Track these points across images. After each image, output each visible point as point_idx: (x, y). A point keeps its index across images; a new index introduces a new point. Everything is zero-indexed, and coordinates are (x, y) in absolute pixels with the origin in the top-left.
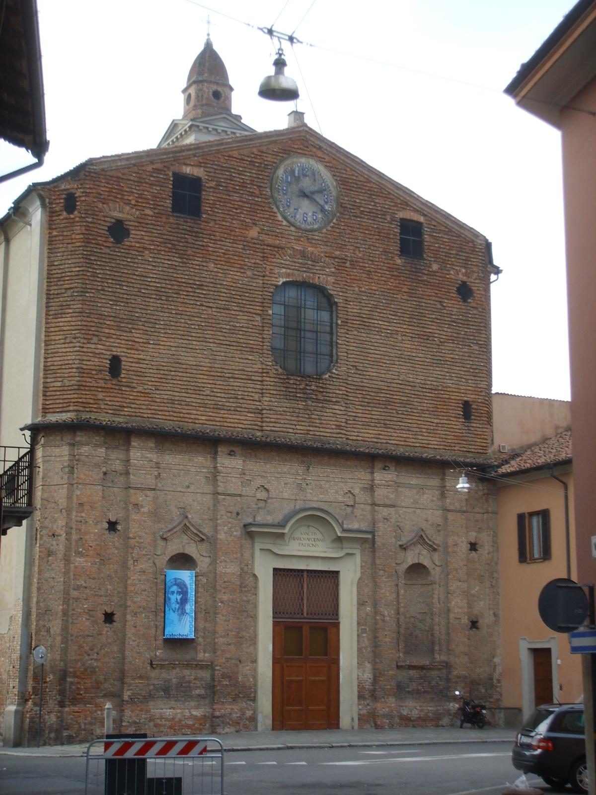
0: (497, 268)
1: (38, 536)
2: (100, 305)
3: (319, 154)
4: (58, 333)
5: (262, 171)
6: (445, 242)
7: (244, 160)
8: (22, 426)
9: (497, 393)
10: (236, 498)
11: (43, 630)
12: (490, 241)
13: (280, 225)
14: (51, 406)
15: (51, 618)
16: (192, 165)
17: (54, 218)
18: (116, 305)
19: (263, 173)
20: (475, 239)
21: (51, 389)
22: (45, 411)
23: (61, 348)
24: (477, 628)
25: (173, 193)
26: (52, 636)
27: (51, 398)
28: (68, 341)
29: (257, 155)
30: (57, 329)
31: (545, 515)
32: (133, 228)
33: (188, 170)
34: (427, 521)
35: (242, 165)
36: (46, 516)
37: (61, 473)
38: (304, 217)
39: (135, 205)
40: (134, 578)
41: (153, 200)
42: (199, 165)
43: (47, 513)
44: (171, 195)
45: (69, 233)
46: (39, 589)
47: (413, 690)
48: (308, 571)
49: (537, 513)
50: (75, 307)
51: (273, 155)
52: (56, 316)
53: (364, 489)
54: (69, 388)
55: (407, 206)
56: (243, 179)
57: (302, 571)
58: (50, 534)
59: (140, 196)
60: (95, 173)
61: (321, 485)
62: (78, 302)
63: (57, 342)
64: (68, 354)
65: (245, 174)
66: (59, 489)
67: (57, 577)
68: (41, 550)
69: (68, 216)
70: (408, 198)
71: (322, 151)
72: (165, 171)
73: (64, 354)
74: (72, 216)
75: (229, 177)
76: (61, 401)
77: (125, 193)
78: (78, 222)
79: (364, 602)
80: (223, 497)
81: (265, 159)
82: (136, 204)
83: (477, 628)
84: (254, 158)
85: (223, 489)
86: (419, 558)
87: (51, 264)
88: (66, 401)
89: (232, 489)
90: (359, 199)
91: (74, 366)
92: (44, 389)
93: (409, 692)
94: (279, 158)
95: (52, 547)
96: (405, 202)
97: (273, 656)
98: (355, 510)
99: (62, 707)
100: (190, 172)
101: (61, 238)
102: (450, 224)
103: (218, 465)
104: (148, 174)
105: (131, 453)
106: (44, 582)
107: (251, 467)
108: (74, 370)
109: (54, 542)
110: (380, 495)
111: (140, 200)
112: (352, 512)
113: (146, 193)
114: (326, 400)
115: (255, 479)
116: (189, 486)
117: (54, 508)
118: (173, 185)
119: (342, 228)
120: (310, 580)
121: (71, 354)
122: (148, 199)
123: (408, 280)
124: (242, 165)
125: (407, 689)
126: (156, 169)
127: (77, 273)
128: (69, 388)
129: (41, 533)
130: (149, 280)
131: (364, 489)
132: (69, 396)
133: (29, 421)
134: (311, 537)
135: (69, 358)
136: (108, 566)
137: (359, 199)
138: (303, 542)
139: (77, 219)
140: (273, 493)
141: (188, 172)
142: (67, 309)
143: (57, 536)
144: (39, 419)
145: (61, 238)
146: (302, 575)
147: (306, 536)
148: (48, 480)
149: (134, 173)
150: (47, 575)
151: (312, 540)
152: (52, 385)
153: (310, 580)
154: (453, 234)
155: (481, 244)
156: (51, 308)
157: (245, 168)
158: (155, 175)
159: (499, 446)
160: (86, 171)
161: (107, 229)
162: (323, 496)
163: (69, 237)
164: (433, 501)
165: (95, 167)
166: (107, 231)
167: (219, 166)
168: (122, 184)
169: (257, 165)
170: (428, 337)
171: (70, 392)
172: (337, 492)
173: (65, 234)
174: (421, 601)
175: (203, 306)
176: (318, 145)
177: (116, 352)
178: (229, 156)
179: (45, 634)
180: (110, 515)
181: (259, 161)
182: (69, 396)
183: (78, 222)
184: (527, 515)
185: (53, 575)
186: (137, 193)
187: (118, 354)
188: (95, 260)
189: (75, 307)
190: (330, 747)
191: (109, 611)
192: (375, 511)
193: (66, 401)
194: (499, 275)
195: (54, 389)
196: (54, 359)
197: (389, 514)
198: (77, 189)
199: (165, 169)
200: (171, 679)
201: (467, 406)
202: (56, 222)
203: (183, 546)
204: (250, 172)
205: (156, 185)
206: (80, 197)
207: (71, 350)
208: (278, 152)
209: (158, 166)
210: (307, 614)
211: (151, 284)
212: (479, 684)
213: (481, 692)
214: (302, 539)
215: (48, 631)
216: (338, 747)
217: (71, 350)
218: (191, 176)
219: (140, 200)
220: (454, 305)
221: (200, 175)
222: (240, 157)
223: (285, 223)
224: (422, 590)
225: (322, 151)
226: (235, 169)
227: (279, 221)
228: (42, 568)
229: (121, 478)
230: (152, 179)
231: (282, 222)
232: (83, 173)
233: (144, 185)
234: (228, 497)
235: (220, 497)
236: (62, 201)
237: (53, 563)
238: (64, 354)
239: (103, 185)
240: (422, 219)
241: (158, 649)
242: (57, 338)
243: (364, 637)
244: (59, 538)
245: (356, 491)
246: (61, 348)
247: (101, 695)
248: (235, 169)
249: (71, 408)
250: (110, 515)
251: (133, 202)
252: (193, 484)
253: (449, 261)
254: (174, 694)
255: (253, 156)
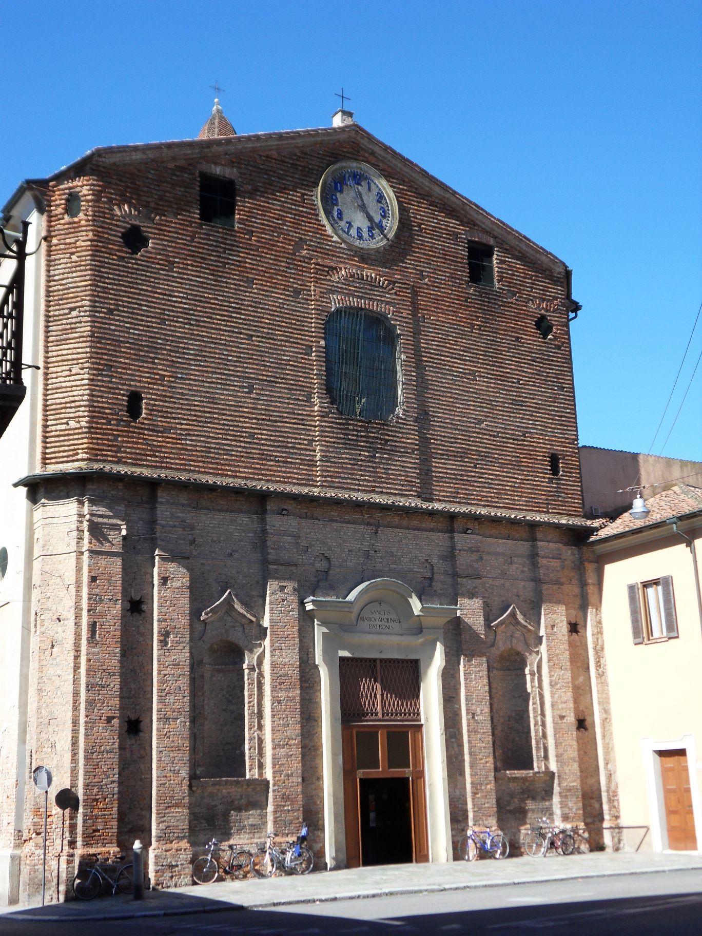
0: (576, 303)
1: (38, 622)
2: (113, 328)
3: (371, 158)
4: (60, 364)
5: (306, 176)
6: (519, 268)
7: (285, 162)
8: (16, 480)
9: (584, 447)
10: (291, 568)
11: (46, 746)
12: (570, 269)
13: (330, 241)
14: (53, 455)
15: (56, 729)
16: (223, 165)
17: (53, 224)
18: (134, 329)
19: (308, 179)
20: (552, 266)
21: (53, 433)
22: (45, 461)
23: (65, 382)
24: (586, 729)
25: (201, 196)
26: (58, 753)
27: (53, 445)
28: (74, 372)
29: (300, 157)
30: (60, 358)
31: (665, 583)
32: (153, 236)
33: (218, 170)
34: (517, 596)
35: (283, 168)
36: (48, 595)
37: (67, 539)
38: (358, 232)
39: (155, 209)
40: (165, 672)
41: (176, 204)
42: (231, 164)
43: (50, 591)
44: (199, 198)
45: (72, 240)
46: (40, 691)
47: (515, 808)
48: (381, 660)
49: (656, 582)
50: (82, 329)
51: (318, 158)
52: (59, 342)
53: (443, 558)
54: (76, 431)
55: (474, 225)
56: (284, 184)
57: (375, 660)
58: (55, 618)
59: (161, 198)
60: (104, 167)
61: (392, 553)
62: (86, 324)
63: (59, 374)
64: (74, 388)
65: (287, 178)
66: (65, 559)
67: (63, 674)
68: (42, 639)
69: (71, 220)
70: (476, 216)
71: (375, 157)
72: (190, 170)
73: (69, 389)
74: (76, 219)
75: (267, 181)
76: (66, 448)
77: (142, 193)
78: (84, 226)
79: (451, 697)
80: (276, 567)
81: (310, 162)
82: (157, 207)
83: (586, 729)
84: (296, 159)
85: (275, 557)
86: (511, 642)
87: (49, 279)
88: (72, 448)
89: (285, 556)
90: (420, 215)
91: (82, 403)
92: (44, 434)
93: (510, 812)
94: (325, 162)
95: (56, 635)
96: (472, 221)
97: (344, 767)
98: (434, 584)
99: (73, 849)
100: (220, 172)
101: (62, 247)
102: (524, 248)
103: (268, 527)
104: (170, 171)
105: (158, 512)
106: (46, 681)
107: (308, 530)
108: (83, 409)
109: (60, 628)
110: (463, 565)
111: (160, 203)
112: (430, 586)
113: (168, 194)
114: (392, 451)
115: (313, 545)
116: (231, 554)
117: (58, 584)
118: (200, 187)
119: (403, 247)
120: (384, 671)
121: (79, 388)
122: (171, 202)
123: (480, 311)
124: (283, 168)
125: (508, 808)
126: (179, 166)
127: (83, 289)
128: (76, 431)
129: (42, 617)
130: (174, 299)
131: (443, 558)
132: (76, 442)
133: (24, 473)
134: (384, 617)
135: (75, 393)
136: (130, 658)
137: (420, 215)
138: (375, 623)
139: (83, 223)
140: (334, 561)
141: (218, 173)
142: (72, 333)
143: (64, 620)
144: (38, 471)
145: (62, 247)
146: (375, 666)
147: (378, 616)
148: (51, 548)
149: (152, 169)
150: (51, 671)
151: (386, 620)
152: (53, 428)
153: (384, 671)
154: (528, 259)
155: (560, 273)
156: (51, 334)
157: (286, 171)
158: (178, 173)
159: (591, 508)
160: (93, 165)
161: (120, 235)
162: (396, 566)
163: (73, 245)
164: (523, 572)
165: (104, 159)
166: (121, 237)
167: (255, 167)
168: (137, 183)
169: (300, 168)
170: (505, 378)
171: (76, 437)
172: (411, 561)
173: (68, 241)
174: (516, 696)
175: (241, 333)
176: (370, 149)
177: (135, 385)
178: (267, 157)
179: (50, 750)
180: (133, 591)
181: (302, 164)
182: (76, 442)
183: (84, 226)
184: (640, 586)
185: (59, 672)
186: (156, 194)
187: (139, 389)
188: (106, 273)
189: (82, 329)
190: (442, 890)
191: (133, 718)
192: (457, 584)
193: (72, 448)
194: (578, 312)
195: (57, 433)
196: (56, 396)
197: (475, 587)
198: (82, 187)
199: (190, 167)
200: (216, 806)
201: (554, 460)
202: (56, 228)
203: (227, 631)
204: (292, 177)
205: (180, 186)
206: (85, 195)
207: (78, 383)
208: (324, 155)
209: (181, 163)
210: (383, 715)
211: (177, 305)
212: (592, 798)
213: (595, 808)
214: (373, 619)
215: (53, 746)
216: (451, 889)
217: (78, 383)
218: (221, 178)
219: (160, 203)
220: (531, 340)
221: (233, 177)
222: (279, 159)
223: (335, 238)
224: (516, 682)
225: (375, 157)
226: (274, 172)
227: (328, 236)
228: (44, 663)
229: (146, 545)
230: (174, 178)
231: (333, 237)
232: (89, 166)
233: (165, 185)
234: (280, 567)
235: (271, 567)
236: (63, 202)
237: (58, 656)
238: (69, 389)
239: (113, 181)
240: (491, 242)
241: (199, 766)
242: (59, 369)
243: (453, 742)
244: (66, 622)
245: (435, 560)
246: (65, 382)
247: (126, 830)
248: (274, 172)
249: (79, 457)
250: (133, 591)
251: (152, 205)
252: (237, 551)
253: (524, 290)
254: (220, 825)
255: (295, 158)
